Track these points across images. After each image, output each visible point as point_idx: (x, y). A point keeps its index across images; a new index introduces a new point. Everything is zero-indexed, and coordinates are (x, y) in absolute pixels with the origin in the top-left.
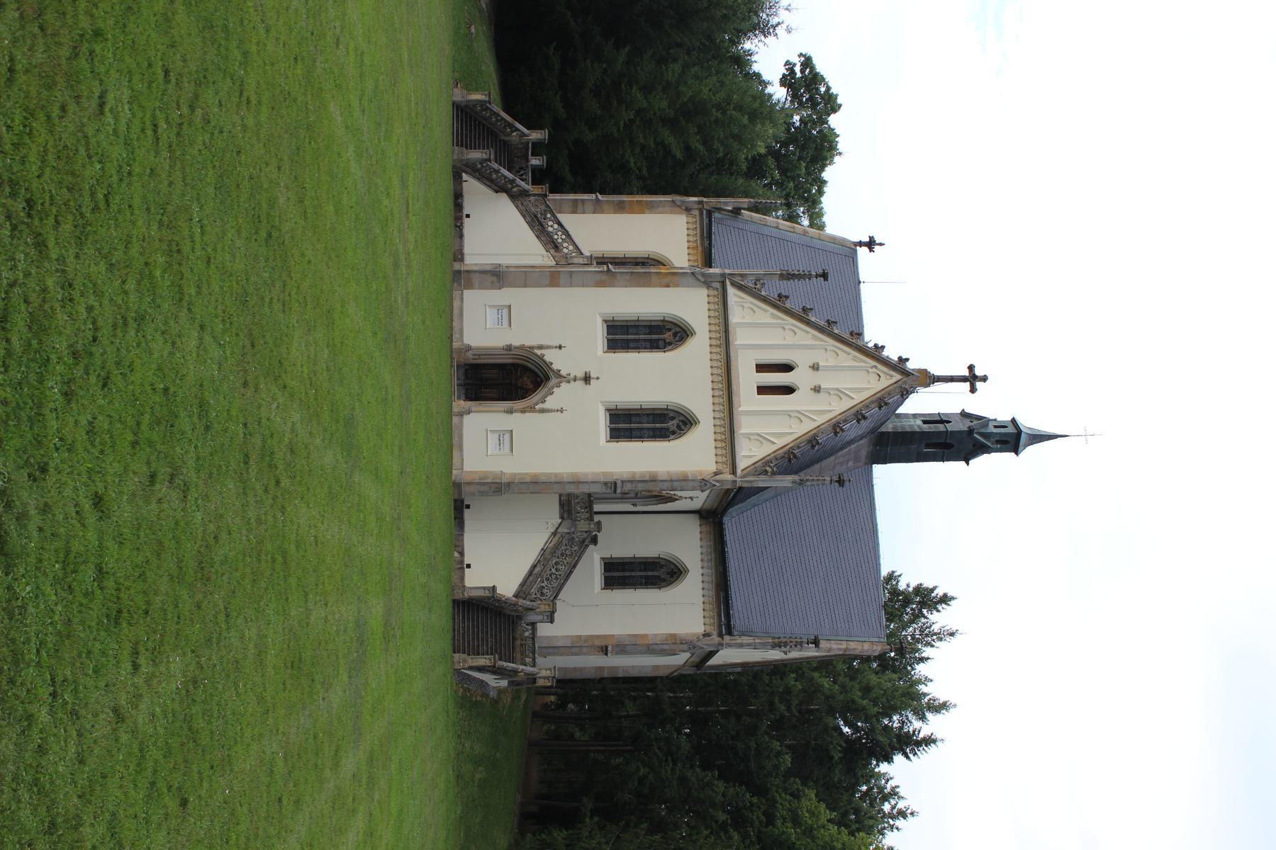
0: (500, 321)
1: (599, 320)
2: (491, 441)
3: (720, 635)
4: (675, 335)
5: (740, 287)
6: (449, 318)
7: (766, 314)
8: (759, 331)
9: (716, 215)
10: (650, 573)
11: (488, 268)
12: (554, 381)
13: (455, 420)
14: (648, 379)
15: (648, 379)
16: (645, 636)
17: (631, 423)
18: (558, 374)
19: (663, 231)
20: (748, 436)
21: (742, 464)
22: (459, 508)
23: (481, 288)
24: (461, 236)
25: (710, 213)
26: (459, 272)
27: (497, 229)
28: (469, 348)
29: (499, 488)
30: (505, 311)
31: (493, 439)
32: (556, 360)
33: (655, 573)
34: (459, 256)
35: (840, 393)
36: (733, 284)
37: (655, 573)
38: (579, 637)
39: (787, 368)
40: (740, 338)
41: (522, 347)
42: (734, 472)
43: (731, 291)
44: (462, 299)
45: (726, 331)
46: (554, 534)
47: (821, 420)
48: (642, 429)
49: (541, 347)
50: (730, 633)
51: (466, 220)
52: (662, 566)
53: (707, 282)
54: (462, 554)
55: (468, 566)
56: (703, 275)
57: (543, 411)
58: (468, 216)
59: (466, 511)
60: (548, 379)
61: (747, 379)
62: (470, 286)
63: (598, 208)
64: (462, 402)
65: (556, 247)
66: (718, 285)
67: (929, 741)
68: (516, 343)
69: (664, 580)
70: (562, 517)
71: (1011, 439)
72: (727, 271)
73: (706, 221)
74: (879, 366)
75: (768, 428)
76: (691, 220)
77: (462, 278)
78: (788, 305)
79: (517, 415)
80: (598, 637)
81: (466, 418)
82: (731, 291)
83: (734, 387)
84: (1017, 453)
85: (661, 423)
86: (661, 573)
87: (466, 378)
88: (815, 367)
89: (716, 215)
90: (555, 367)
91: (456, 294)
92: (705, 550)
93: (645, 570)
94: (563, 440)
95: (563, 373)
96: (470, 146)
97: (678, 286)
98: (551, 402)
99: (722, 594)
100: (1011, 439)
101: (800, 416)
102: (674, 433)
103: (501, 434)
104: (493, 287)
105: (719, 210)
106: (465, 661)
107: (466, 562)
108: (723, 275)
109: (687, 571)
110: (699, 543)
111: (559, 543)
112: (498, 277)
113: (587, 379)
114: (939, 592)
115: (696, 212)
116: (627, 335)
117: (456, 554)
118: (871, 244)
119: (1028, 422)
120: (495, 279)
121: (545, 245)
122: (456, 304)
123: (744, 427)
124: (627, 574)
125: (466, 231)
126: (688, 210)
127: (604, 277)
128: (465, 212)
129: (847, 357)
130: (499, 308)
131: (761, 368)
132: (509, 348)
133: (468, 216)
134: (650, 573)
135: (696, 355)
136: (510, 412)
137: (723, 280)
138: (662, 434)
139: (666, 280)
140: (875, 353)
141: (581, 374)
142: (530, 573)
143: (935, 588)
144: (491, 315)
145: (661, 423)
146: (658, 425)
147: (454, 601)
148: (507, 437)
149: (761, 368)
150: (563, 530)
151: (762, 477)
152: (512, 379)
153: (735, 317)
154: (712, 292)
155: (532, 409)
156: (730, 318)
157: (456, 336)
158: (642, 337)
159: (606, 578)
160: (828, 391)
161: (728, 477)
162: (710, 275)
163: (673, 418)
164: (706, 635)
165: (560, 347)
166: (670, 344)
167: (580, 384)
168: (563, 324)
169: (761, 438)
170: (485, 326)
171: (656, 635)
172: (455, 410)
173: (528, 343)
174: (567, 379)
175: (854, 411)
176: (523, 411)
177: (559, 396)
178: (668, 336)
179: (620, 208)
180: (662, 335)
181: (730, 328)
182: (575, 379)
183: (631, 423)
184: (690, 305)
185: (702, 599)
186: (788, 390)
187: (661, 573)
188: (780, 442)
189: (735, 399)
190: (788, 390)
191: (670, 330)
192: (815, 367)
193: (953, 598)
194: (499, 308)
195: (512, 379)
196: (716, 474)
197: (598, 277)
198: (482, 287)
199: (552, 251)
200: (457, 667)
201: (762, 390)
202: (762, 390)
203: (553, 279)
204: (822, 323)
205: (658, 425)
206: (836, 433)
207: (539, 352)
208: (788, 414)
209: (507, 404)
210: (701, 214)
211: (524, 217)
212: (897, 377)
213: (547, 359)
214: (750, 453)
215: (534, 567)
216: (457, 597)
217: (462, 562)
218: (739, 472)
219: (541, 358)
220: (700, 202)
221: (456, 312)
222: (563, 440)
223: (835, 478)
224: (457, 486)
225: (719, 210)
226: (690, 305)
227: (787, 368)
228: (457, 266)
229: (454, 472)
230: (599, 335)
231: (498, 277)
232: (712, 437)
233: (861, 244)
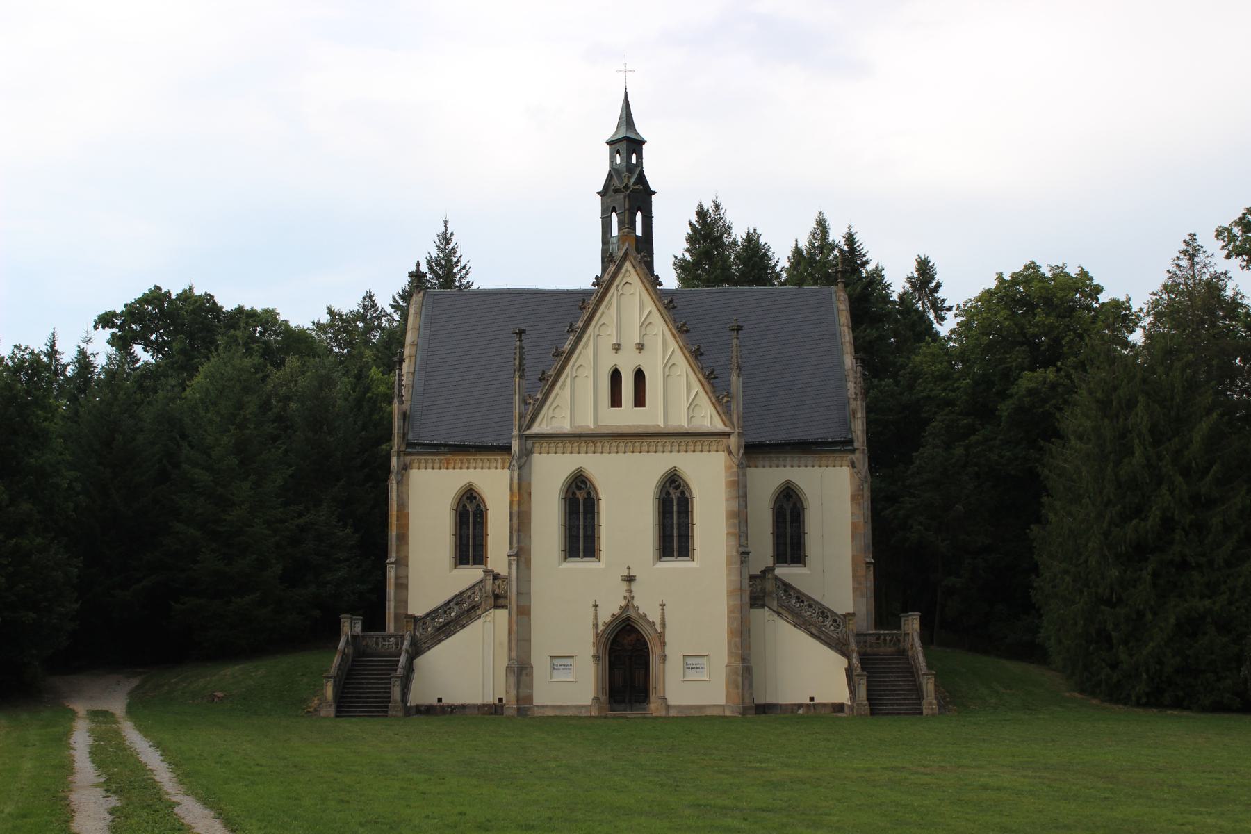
0: (567, 668)
1: (566, 565)
2: (693, 677)
3: (853, 451)
4: (579, 488)
5: (533, 420)
6: (564, 722)
7: (562, 394)
8: (577, 401)
9: (410, 437)
10: (788, 518)
11: (513, 679)
12: (631, 613)
13: (673, 713)
14: (627, 516)
15: (627, 516)
16: (854, 525)
17: (674, 536)
18: (624, 609)
19: (427, 497)
20: (690, 419)
21: (719, 426)
22: (764, 709)
24: (463, 707)
25: (410, 445)
26: (519, 709)
27: (462, 668)
28: (596, 699)
29: (745, 667)
30: (556, 662)
31: (692, 675)
32: (610, 609)
33: (788, 513)
34: (495, 710)
35: (645, 324)
36: (529, 427)
37: (788, 513)
38: (855, 590)
39: (616, 376)
40: (587, 422)
41: (596, 645)
42: (728, 435)
43: (535, 429)
44: (543, 706)
45: (580, 436)
46: (779, 614)
47: (673, 345)
48: (679, 525)
49: (596, 626)
50: (851, 442)
51: (444, 702)
52: (781, 506)
53: (526, 453)
54: (800, 706)
55: (812, 699)
56: (520, 458)
57: (663, 625)
59: (816, 701)
60: (628, 619)
61: (628, 417)
62: (530, 698)
63: (402, 562)
64: (652, 706)
65: (474, 608)
66: (529, 443)
67: (850, 239)
68: (591, 651)
69: (795, 504)
70: (763, 606)
71: (628, 144)
72: (516, 432)
73: (419, 449)
74: (616, 283)
75: (680, 397)
76: (416, 465)
77: (524, 705)
78: (552, 372)
79: (668, 651)
80: (855, 571)
81: (672, 701)
82: (535, 429)
83: (639, 430)
84: (644, 142)
85: (674, 505)
86: (788, 507)
87: (624, 701)
88: (617, 347)
89: (410, 437)
90: (617, 611)
91: (538, 713)
92: (767, 463)
93: (785, 522)
94: (693, 606)
95: (623, 603)
96: (388, 699)
97: (529, 484)
98: (654, 616)
99: (814, 448)
100: (628, 144)
101: (669, 366)
102: (683, 493)
103: (687, 667)
104: (530, 675)
105: (405, 435)
106: (931, 703)
107: (808, 701)
108: (521, 436)
109: (788, 482)
110: (760, 469)
111: (788, 609)
112: (520, 670)
113: (630, 579)
114: (694, 218)
115: (408, 459)
116: (581, 537)
117: (800, 712)
119: (610, 128)
121: (471, 620)
122: (550, 713)
123: (680, 421)
124: (788, 541)
125: (457, 702)
126: (406, 467)
127: (523, 559)
128: (435, 702)
129: (608, 314)
130: (553, 668)
131: (616, 401)
132: (596, 658)
133: (440, 700)
134: (788, 518)
135: (603, 468)
136: (664, 657)
137: (524, 437)
138: (685, 504)
139: (525, 495)
140: (604, 285)
141: (624, 586)
142: (818, 638)
143: (690, 223)
144: (560, 676)
145: (674, 505)
146: (675, 508)
147: (872, 714)
148: (689, 661)
149: (616, 401)
150: (775, 605)
151: (733, 406)
152: (627, 654)
153: (566, 427)
154: (537, 448)
155: (661, 636)
156: (566, 431)
157: (584, 713)
158: (581, 523)
159: (793, 562)
160: (643, 336)
161: (733, 441)
162: (521, 450)
163: (668, 493)
164: (853, 465)
165: (596, 606)
166: (589, 494)
167: (634, 586)
168: (571, 605)
169: (692, 406)
170: (572, 683)
171: (853, 514)
172: (663, 713)
173: (590, 638)
174: (630, 599)
175: (665, 312)
176: (664, 644)
177: (647, 607)
178: (581, 496)
179: (403, 538)
180: (580, 503)
181: (578, 431)
182: (630, 591)
183: (674, 536)
184: (551, 472)
185: (816, 468)
186: (639, 376)
187: (788, 507)
188: (696, 387)
189: (652, 430)
190: (639, 376)
191: (574, 493)
192: (617, 347)
193: (701, 206)
194: (553, 668)
195: (627, 654)
196: (730, 453)
198: (531, 686)
199: (479, 612)
200: (936, 711)
201: (639, 401)
202: (639, 401)
203: (524, 612)
204: (572, 338)
205: (675, 508)
206: (687, 331)
207: (601, 628)
208: (666, 377)
209: (654, 660)
210: (410, 454)
211: (440, 641)
212: (628, 265)
213: (608, 619)
214: (708, 418)
215: (812, 635)
216: (868, 711)
217: (808, 706)
218: (728, 430)
219: (607, 625)
220: (399, 454)
221: (557, 713)
222: (693, 606)
223: (734, 334)
224: (745, 711)
225: (405, 435)
226: (551, 472)
227: (616, 376)
228: (513, 712)
229: (728, 713)
230: (580, 565)
231: (520, 670)
232: (690, 454)
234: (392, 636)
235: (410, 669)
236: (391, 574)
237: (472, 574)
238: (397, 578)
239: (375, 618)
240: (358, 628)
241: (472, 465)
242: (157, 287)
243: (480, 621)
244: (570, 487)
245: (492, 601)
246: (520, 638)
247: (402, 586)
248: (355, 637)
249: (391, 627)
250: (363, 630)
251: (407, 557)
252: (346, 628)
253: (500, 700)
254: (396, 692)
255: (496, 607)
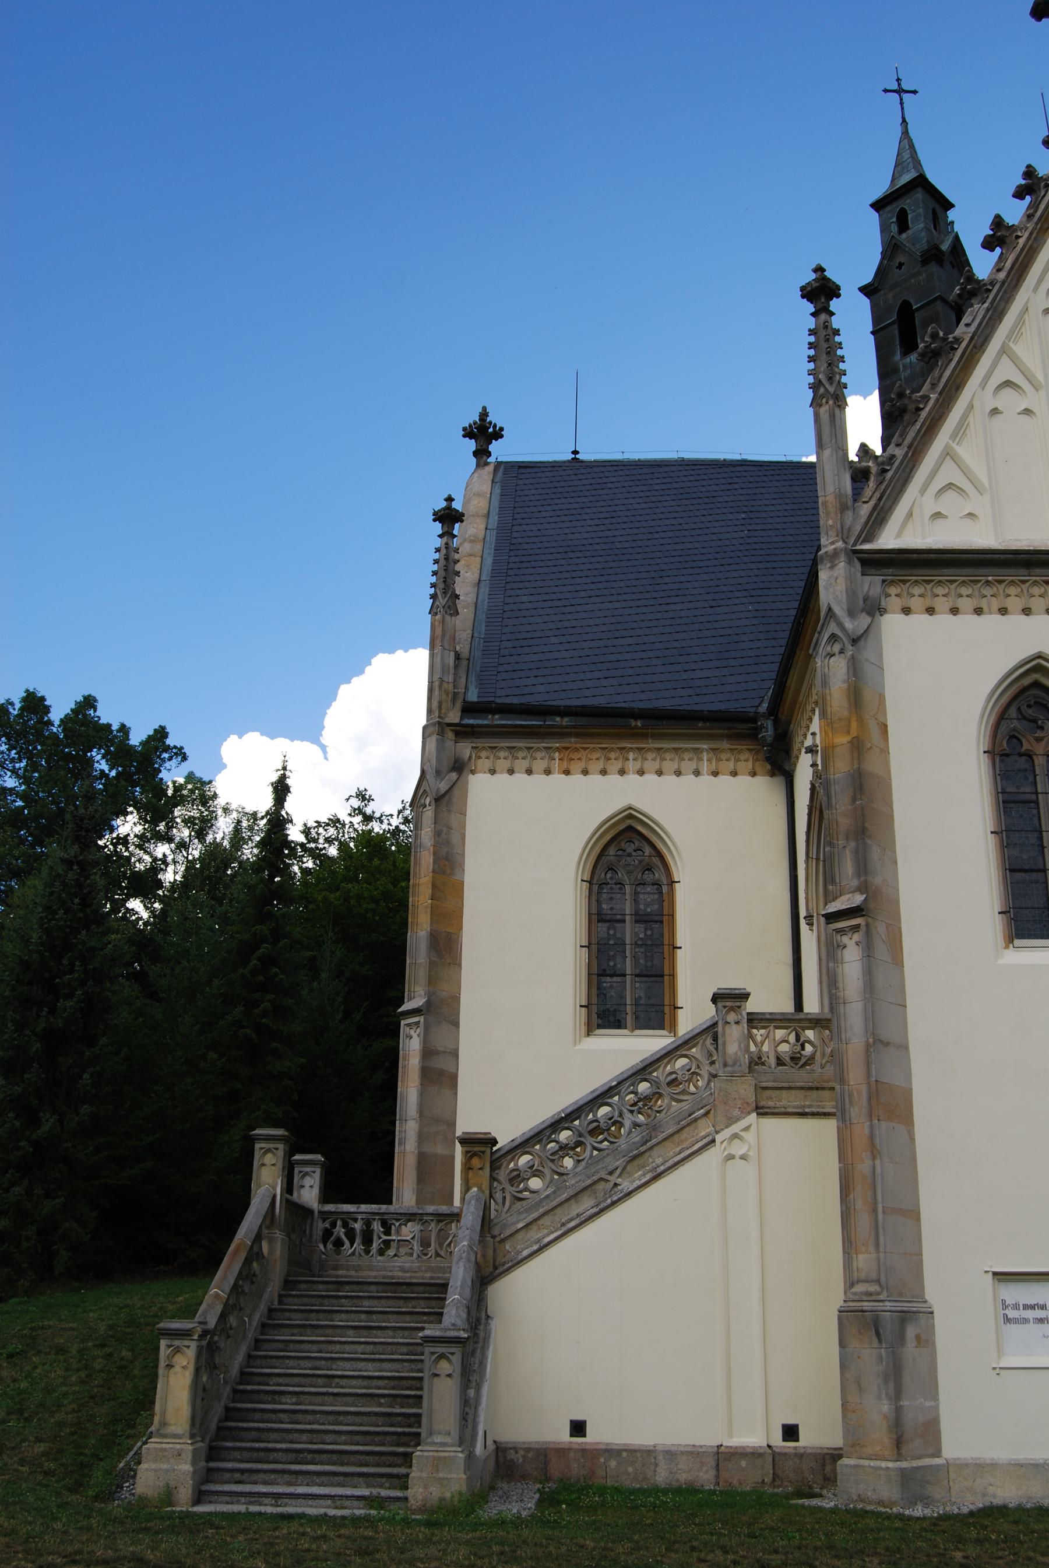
5: (878, 519)
23: (932, 1390)
25: (468, 709)
30: (1014, 1293)
43: (888, 539)
51: (593, 1436)
58: (578, 1428)
62: (931, 1430)
63: (443, 1011)
104: (926, 1341)
115: (465, 749)
118: (483, 433)
120: (911, 1331)
128: (564, 1436)
133: (578, 1428)
179: (446, 947)
197: (882, 951)
233: (482, 453)
234: (411, 1217)
235: (478, 1314)
236: (412, 1045)
237: (634, 1046)
238: (428, 1052)
239: (361, 1166)
240: (309, 1193)
241: (631, 765)
242: (43, 699)
243: (712, 1157)
244: (1002, 717)
245: (745, 1088)
246: (876, 1204)
247: (441, 1076)
248: (298, 1212)
249: (406, 1194)
250: (328, 1194)
251: (456, 999)
252: (267, 1177)
253: (790, 1432)
254: (442, 1396)
255: (762, 1112)
